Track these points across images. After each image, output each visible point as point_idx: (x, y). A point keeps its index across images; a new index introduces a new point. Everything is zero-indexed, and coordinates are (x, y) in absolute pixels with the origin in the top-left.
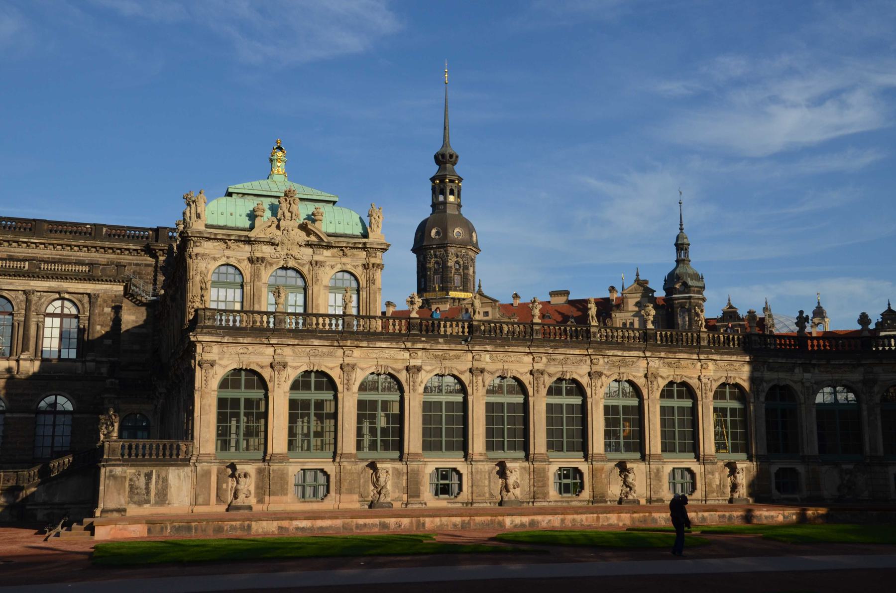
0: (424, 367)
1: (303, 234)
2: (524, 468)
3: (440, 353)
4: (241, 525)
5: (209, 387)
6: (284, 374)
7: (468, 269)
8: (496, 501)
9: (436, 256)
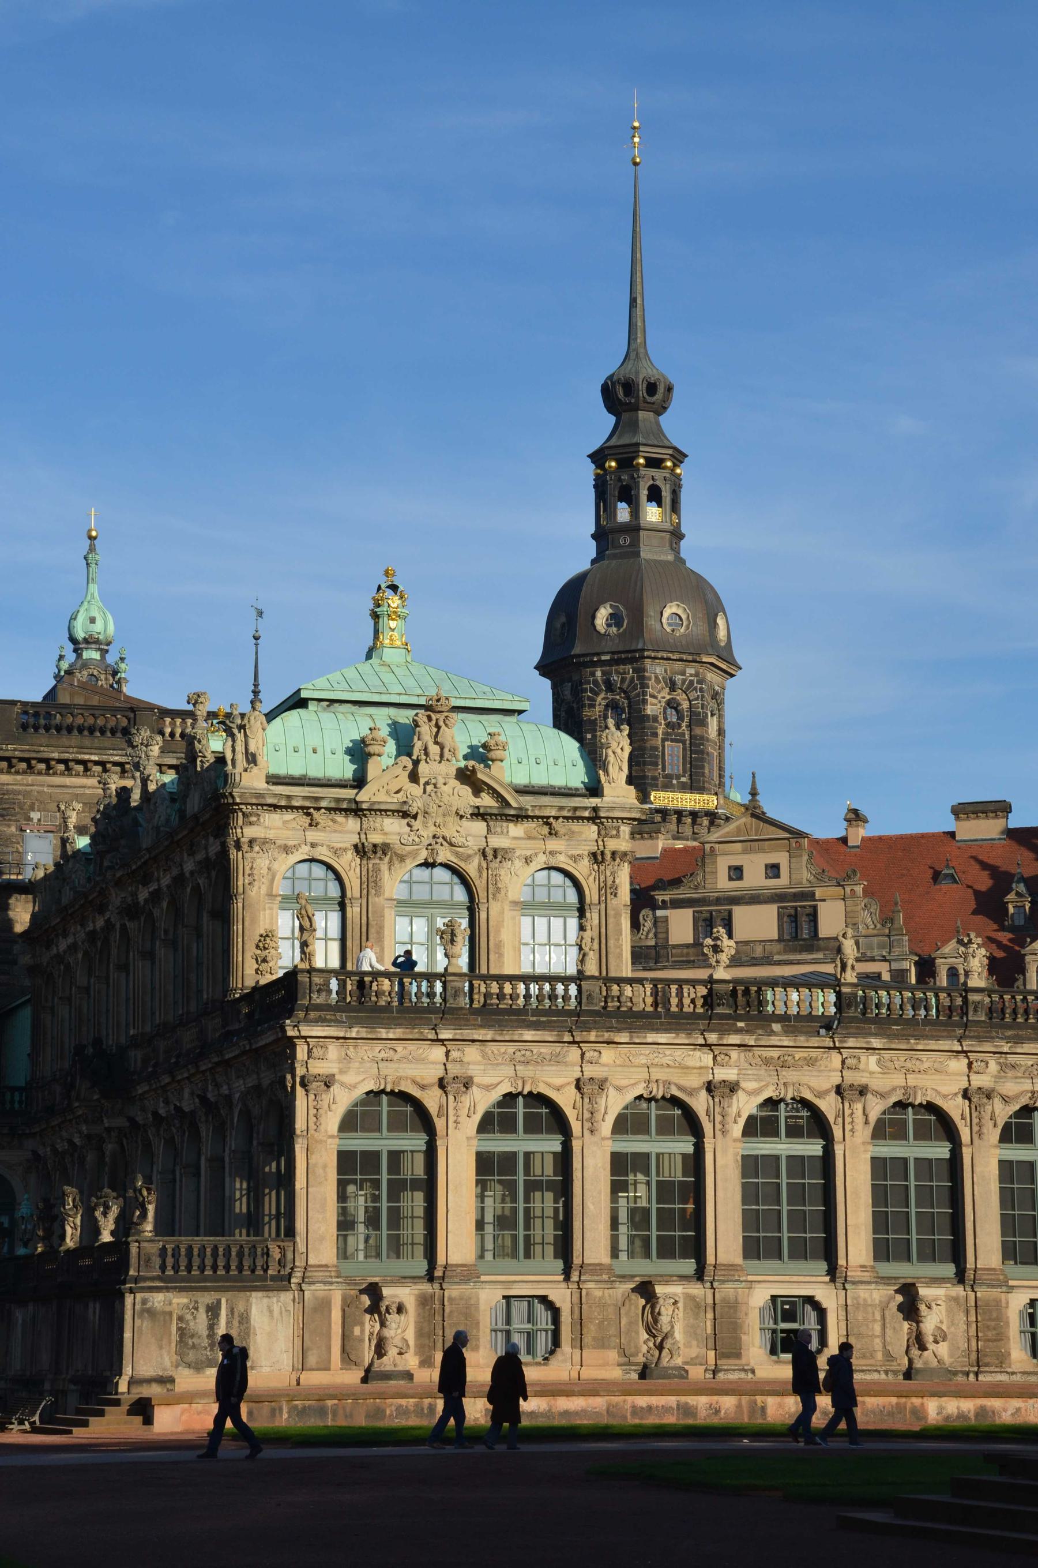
0: (743, 1084)
1: (466, 791)
2: (956, 1299)
3: (775, 1053)
4: (416, 1405)
5: (322, 1128)
6: (466, 1100)
7: (703, 723)
8: (899, 1368)
9: (610, 687)
